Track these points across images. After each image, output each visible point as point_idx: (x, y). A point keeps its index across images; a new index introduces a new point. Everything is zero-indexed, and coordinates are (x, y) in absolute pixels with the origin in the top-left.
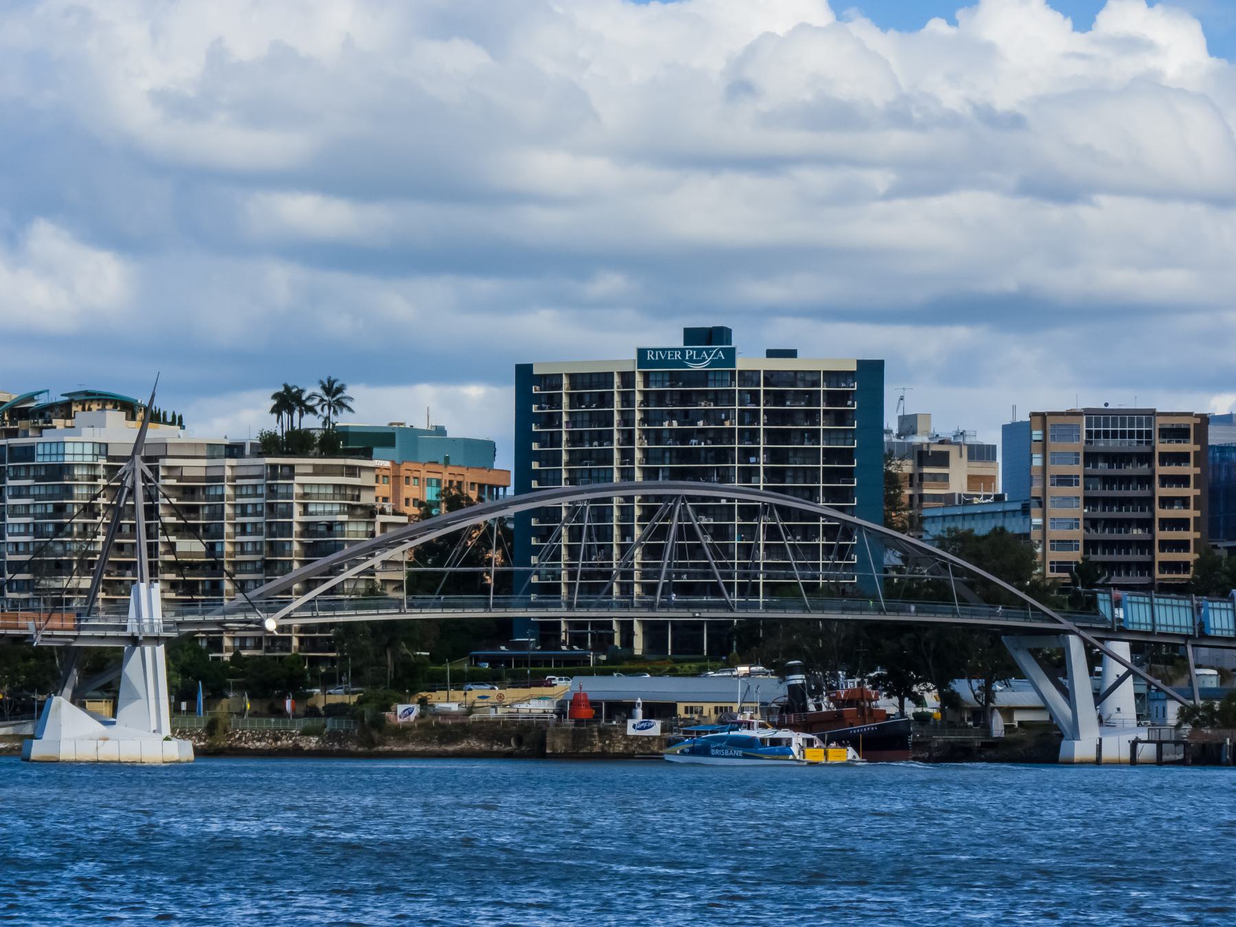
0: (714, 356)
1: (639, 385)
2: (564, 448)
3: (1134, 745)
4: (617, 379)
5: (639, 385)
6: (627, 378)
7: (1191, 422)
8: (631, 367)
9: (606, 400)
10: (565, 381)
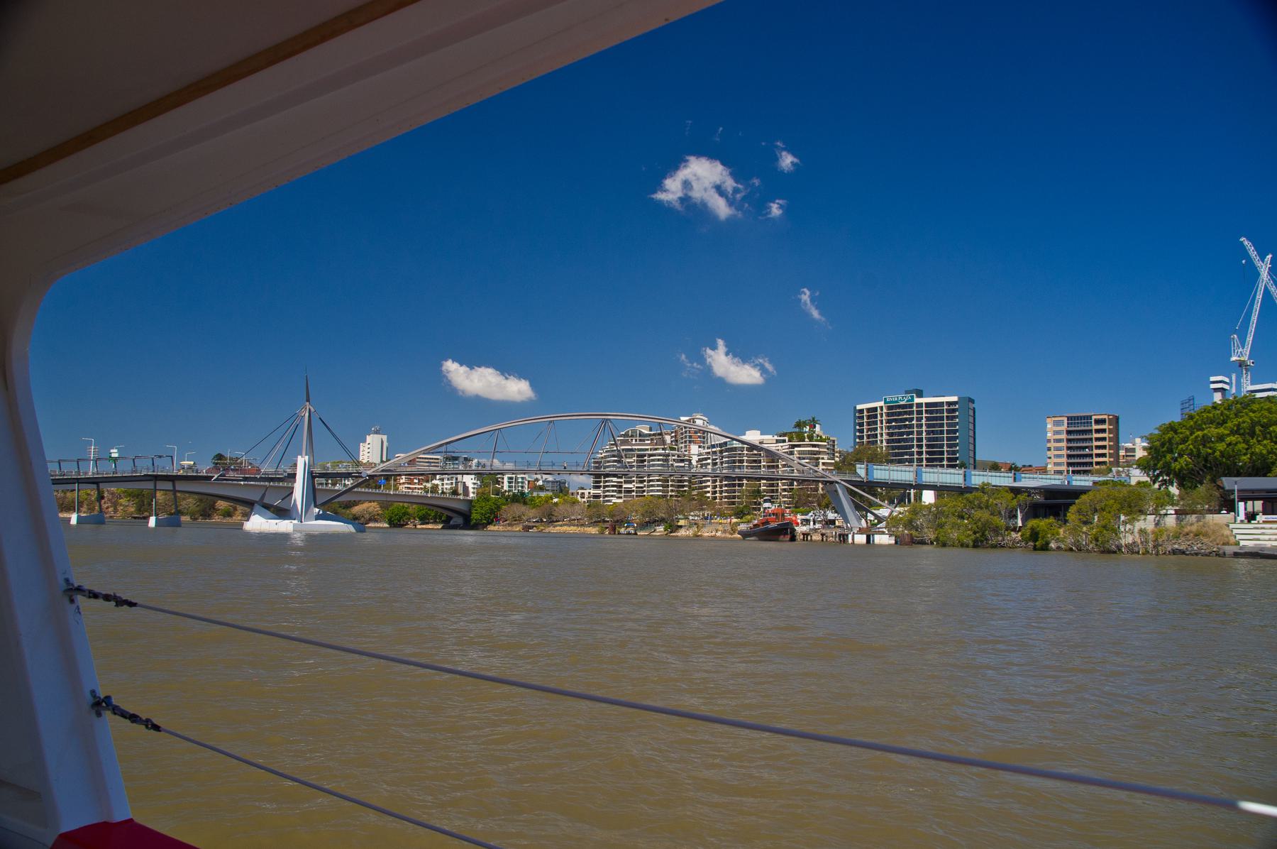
1: (885, 410)
2: (865, 433)
5: (885, 410)
6: (881, 408)
7: (1106, 417)
8: (881, 403)
9: (876, 416)
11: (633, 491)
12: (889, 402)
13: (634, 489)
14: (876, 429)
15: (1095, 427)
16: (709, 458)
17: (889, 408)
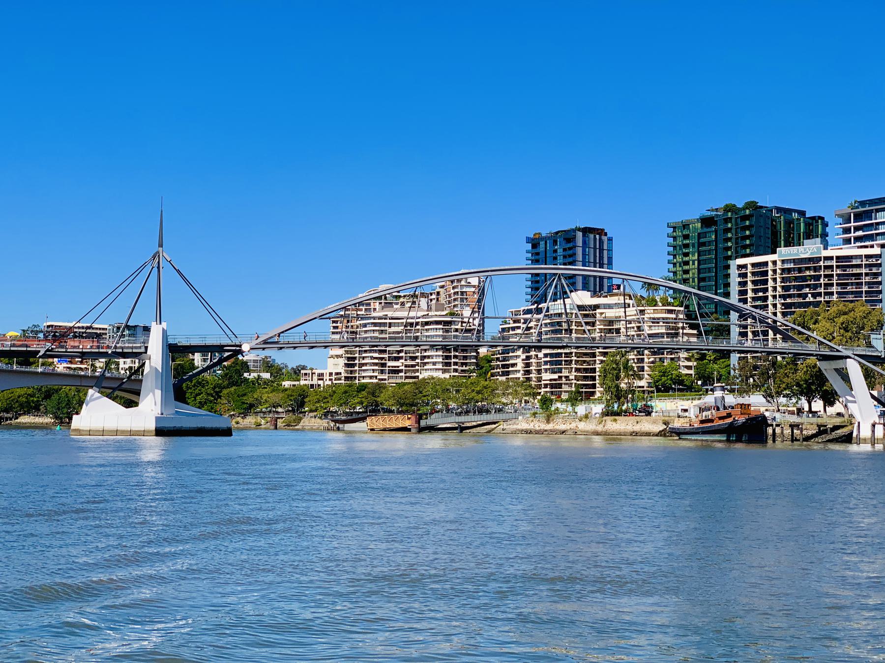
0: (813, 250)
3: (874, 426)
4: (770, 264)
9: (765, 273)
10: (749, 267)
11: (401, 371)
12: (785, 255)
13: (403, 368)
14: (766, 290)
16: (519, 328)
17: (783, 262)
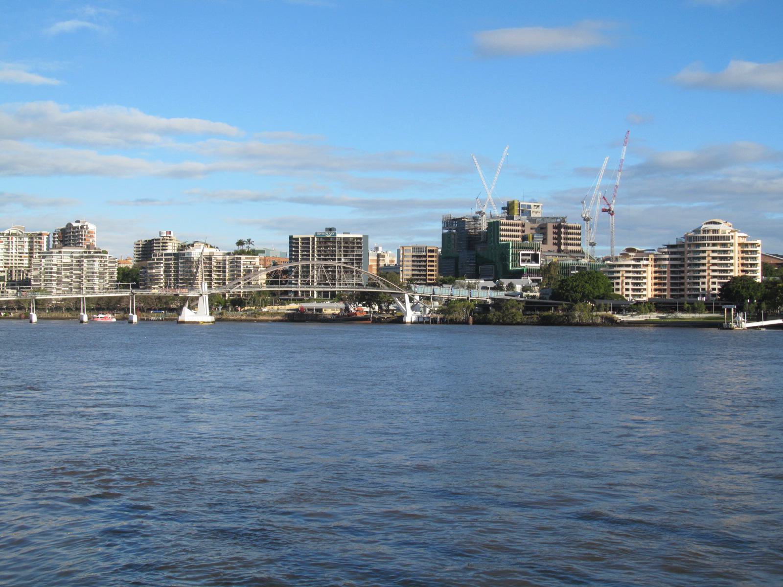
6: (313, 239)
7: (435, 249)
10: (300, 239)
14: (309, 251)
15: (428, 254)
16: (162, 263)
17: (319, 239)
